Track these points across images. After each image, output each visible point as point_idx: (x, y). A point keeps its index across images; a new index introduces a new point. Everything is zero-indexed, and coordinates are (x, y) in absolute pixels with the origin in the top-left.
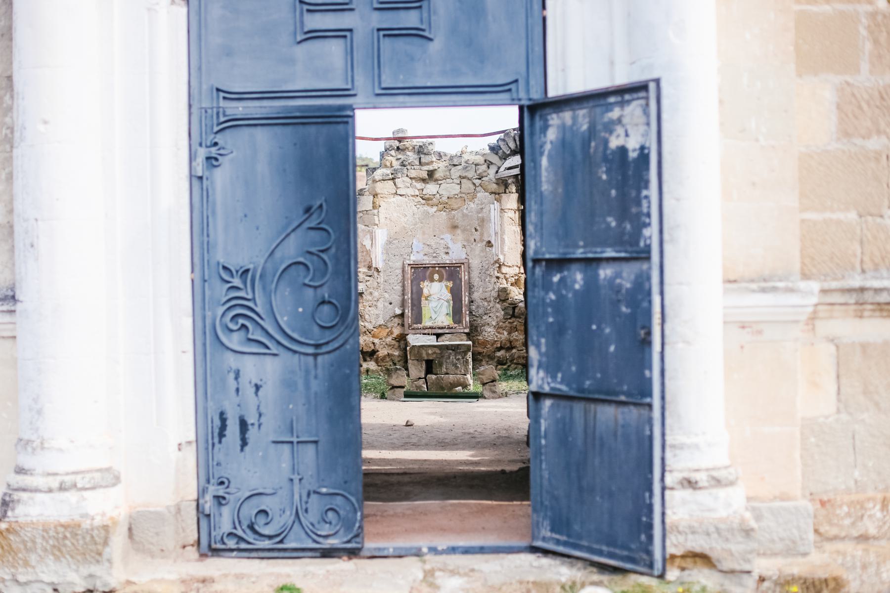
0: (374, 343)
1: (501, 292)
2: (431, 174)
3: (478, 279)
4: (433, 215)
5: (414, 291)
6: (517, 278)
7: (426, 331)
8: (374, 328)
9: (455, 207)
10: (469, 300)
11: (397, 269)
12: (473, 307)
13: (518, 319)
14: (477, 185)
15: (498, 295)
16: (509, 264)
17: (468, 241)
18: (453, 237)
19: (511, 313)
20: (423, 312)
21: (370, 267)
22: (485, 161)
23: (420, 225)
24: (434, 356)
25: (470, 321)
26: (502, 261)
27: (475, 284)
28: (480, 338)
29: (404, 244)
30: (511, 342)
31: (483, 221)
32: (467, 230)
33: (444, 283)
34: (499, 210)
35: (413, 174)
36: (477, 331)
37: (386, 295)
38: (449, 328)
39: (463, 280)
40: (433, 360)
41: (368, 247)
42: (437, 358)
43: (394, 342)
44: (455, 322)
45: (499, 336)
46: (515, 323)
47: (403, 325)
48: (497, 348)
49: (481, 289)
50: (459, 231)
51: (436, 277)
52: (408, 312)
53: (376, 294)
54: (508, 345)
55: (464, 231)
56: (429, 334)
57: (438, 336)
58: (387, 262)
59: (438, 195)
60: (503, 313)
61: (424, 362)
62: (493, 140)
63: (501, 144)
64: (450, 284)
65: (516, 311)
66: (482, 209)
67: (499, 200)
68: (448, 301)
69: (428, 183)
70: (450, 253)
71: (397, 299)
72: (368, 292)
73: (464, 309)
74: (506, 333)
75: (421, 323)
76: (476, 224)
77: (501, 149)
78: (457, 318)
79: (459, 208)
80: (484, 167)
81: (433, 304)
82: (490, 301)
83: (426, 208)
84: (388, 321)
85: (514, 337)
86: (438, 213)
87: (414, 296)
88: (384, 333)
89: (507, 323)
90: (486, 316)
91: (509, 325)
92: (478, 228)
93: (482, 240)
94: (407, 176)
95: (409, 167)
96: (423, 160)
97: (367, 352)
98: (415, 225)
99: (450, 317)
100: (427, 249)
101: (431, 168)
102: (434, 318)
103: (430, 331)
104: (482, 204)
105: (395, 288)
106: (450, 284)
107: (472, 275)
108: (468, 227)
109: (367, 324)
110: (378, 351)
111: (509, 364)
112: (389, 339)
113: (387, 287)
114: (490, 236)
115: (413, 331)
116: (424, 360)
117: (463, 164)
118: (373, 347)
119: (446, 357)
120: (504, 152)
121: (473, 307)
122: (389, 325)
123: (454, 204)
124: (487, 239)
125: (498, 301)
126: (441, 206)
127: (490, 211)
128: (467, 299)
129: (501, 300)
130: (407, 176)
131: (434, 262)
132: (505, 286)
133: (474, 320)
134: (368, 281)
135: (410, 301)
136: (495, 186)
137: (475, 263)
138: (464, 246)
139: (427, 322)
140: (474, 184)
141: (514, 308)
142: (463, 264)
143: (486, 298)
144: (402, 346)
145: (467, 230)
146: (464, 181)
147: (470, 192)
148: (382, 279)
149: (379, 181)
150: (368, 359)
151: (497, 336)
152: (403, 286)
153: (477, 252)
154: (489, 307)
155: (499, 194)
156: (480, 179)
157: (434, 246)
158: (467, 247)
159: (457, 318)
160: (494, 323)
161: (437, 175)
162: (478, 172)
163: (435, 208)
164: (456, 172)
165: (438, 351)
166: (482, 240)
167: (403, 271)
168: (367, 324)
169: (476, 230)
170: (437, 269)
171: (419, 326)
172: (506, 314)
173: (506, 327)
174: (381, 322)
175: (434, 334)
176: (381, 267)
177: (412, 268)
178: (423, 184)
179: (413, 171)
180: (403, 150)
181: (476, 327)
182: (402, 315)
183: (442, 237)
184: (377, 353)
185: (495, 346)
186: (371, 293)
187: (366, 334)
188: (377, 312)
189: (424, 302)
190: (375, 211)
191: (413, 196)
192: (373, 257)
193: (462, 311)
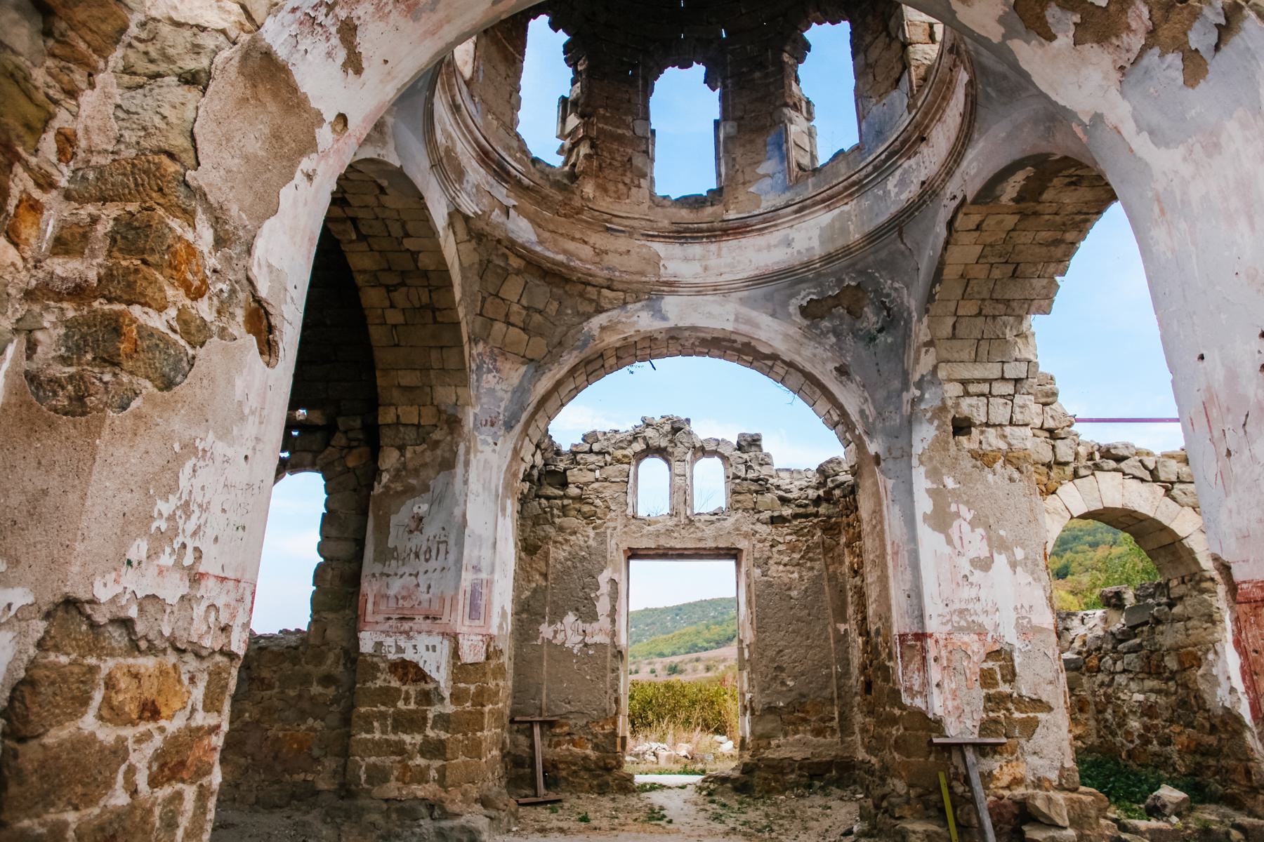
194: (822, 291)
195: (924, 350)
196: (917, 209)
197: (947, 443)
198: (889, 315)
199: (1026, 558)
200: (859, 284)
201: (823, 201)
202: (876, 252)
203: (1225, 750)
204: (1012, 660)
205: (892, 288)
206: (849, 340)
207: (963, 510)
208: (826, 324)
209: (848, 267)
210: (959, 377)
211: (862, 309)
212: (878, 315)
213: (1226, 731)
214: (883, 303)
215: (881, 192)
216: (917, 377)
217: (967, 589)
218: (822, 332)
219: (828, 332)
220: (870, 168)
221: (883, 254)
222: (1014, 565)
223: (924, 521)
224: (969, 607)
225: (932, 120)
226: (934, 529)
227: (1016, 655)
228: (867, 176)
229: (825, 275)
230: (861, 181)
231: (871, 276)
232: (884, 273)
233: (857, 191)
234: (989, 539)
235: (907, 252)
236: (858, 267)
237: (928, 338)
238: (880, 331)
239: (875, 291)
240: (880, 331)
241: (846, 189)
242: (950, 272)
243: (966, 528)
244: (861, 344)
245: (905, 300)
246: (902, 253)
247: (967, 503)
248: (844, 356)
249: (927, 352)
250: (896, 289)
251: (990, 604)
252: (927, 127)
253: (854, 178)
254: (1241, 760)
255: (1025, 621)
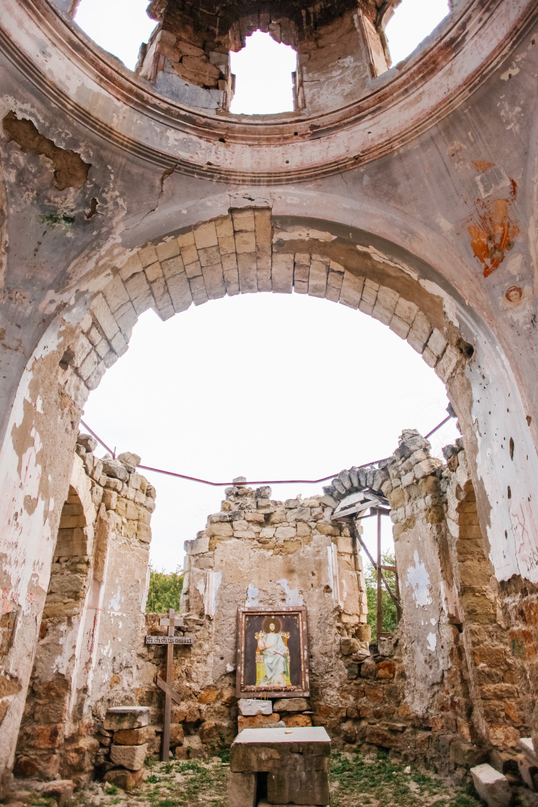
0: (200, 710)
1: (343, 645)
2: (268, 517)
3: (317, 630)
4: (269, 559)
5: (249, 643)
6: (357, 628)
7: (260, 695)
8: (201, 689)
9: (292, 550)
10: (308, 655)
11: (230, 617)
12: (313, 664)
13: (365, 680)
14: (313, 527)
15: (341, 649)
16: (349, 613)
17: (305, 586)
18: (290, 582)
19: (357, 672)
20: (258, 670)
21: (201, 615)
22: (320, 504)
23: (255, 569)
24: (270, 764)
25: (310, 681)
26: (342, 608)
27: (314, 636)
28: (322, 703)
29: (238, 589)
30: (359, 711)
31: (321, 565)
32: (304, 574)
33: (281, 634)
34: (336, 552)
35: (250, 517)
36: (318, 694)
37: (218, 648)
38: (287, 691)
39: (301, 630)
40: (267, 773)
41: (201, 592)
42: (275, 768)
43: (223, 708)
44: (293, 684)
45: (344, 702)
46: (362, 685)
47: (234, 686)
48: (342, 718)
49: (321, 642)
50: (295, 576)
51: (272, 626)
52: (241, 670)
53: (206, 646)
54: (356, 715)
55: (301, 575)
56: (263, 699)
57: (274, 700)
58: (221, 609)
59: (274, 539)
60: (346, 671)
61: (253, 778)
62: (328, 483)
63: (336, 484)
64: (287, 636)
65: (363, 669)
66: (318, 551)
67: (336, 542)
68: (285, 656)
69: (264, 527)
70: (287, 599)
71: (229, 652)
72: (197, 644)
73: (302, 666)
74: (352, 698)
75: (254, 684)
76: (313, 567)
77: (336, 490)
78: (296, 676)
79: (295, 551)
80: (319, 510)
81: (269, 660)
82: (331, 657)
83: (263, 551)
84: (218, 680)
85: (363, 704)
86: (275, 557)
87: (249, 649)
88: (213, 696)
89: (352, 684)
90: (327, 675)
91: (355, 688)
92: (315, 572)
93: (320, 586)
94: (244, 519)
95: (246, 510)
96: (260, 504)
97: (191, 723)
98: (251, 568)
99: (287, 676)
100: (263, 596)
101: (267, 511)
102: (269, 677)
103: (265, 695)
104: (318, 547)
105: (228, 639)
106: (287, 636)
107: (310, 625)
108: (305, 572)
109: (193, 685)
110: (204, 721)
111: (359, 743)
112: (218, 704)
113: (219, 639)
114: (328, 580)
115: (245, 695)
116: (253, 773)
117: (299, 508)
118: (198, 716)
119: (288, 768)
120: (339, 493)
121: (313, 664)
122: (219, 686)
123: (290, 547)
124: (325, 584)
125: (340, 656)
126: (277, 550)
127: (327, 554)
128: (306, 653)
129: (343, 655)
130: (244, 519)
131: (270, 610)
132: (347, 638)
133: (314, 680)
134: (199, 630)
135: (243, 656)
136: (331, 528)
137: (313, 610)
138: (301, 592)
139: (261, 684)
140: (310, 527)
141: (360, 666)
142: (301, 612)
143: (326, 653)
144: (233, 714)
145: (304, 574)
146: (299, 524)
147: (305, 534)
148: (214, 629)
149: (217, 522)
150: (193, 732)
151: (341, 702)
152: (237, 637)
153: (315, 598)
154: (330, 664)
155: (335, 536)
156: (315, 522)
157: (270, 592)
158: (304, 593)
159: (296, 676)
160: (337, 685)
161: (273, 518)
162: (313, 515)
163: (271, 552)
164: (292, 515)
165: (277, 756)
166: (320, 586)
167: (238, 620)
168: (193, 685)
169: (313, 574)
170: (273, 617)
171: (253, 687)
172: (350, 673)
173: (352, 690)
174: (210, 682)
175: (269, 699)
176: (213, 614)
177: (246, 616)
178: (260, 528)
179: (249, 514)
180: (242, 496)
181: (317, 689)
182: (234, 673)
183: (278, 582)
184: (204, 724)
185: (340, 714)
186: (200, 646)
187: (192, 698)
188: (206, 669)
189: (258, 657)
190: (211, 553)
191: (249, 539)
192: (205, 602)
193: (300, 668)
194: (48, 129)
195: (109, 271)
196: (198, 174)
197: (54, 365)
198: (89, 216)
199: (53, 511)
200: (90, 165)
201: (102, 71)
202: (133, 162)
203: (37, 716)
204: (14, 626)
205: (114, 199)
206: (29, 196)
207: (37, 439)
208: (20, 158)
209: (94, 142)
210: (97, 316)
211: (69, 185)
212: (78, 205)
213: (48, 696)
214: (95, 202)
215: (159, 130)
216: (83, 288)
217: (14, 528)
218: (7, 160)
219: (14, 166)
220: (165, 106)
221: (135, 170)
222: (46, 514)
223: (13, 433)
224: (8, 553)
225: (243, 139)
226: (14, 448)
227: (20, 618)
228: (155, 106)
229: (67, 122)
230: (147, 102)
231: (106, 173)
232: (119, 182)
233: (136, 104)
234: (41, 480)
235: (158, 191)
236: (104, 153)
237: (119, 266)
238: (67, 219)
239: (96, 187)
240: (67, 219)
241: (130, 91)
242: (186, 239)
243: (33, 459)
244: (36, 212)
245: (116, 220)
246: (152, 187)
247: (41, 433)
248: (9, 205)
249: (109, 275)
250: (116, 204)
251: (22, 555)
252: (234, 138)
253: (145, 94)
254: (50, 723)
255: (35, 579)
